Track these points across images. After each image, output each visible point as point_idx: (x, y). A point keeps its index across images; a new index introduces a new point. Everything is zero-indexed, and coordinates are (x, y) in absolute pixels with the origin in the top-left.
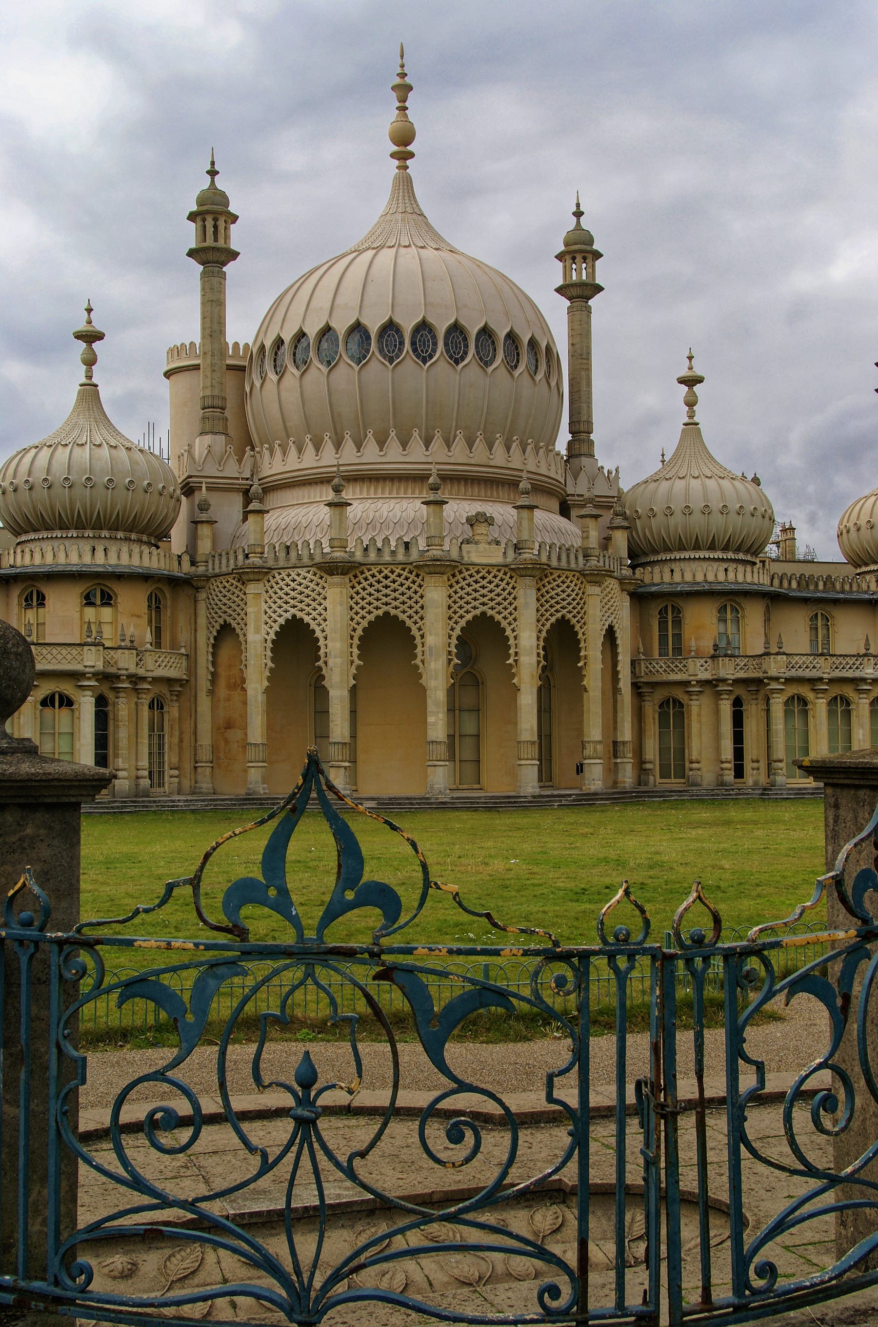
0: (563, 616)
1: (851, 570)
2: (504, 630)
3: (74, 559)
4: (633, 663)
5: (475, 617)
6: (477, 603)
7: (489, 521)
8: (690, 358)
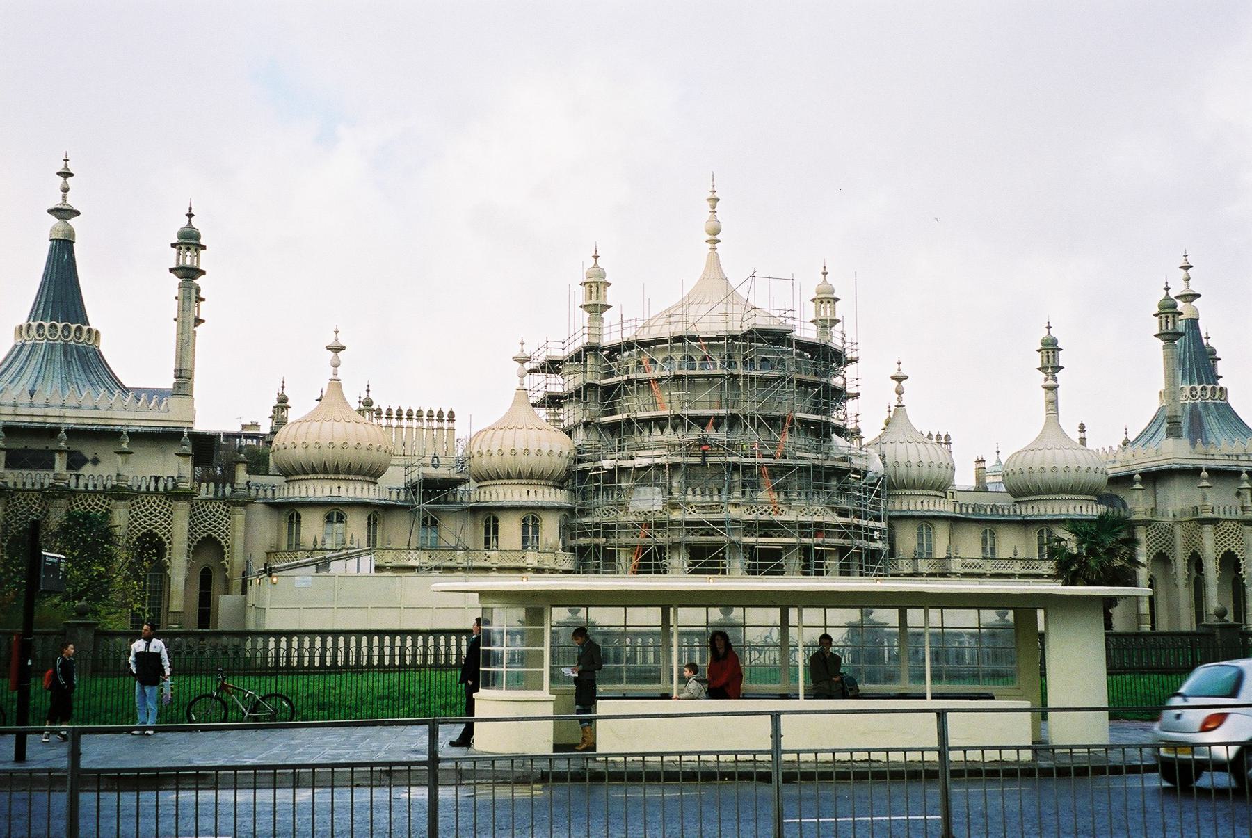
3: (517, 498)
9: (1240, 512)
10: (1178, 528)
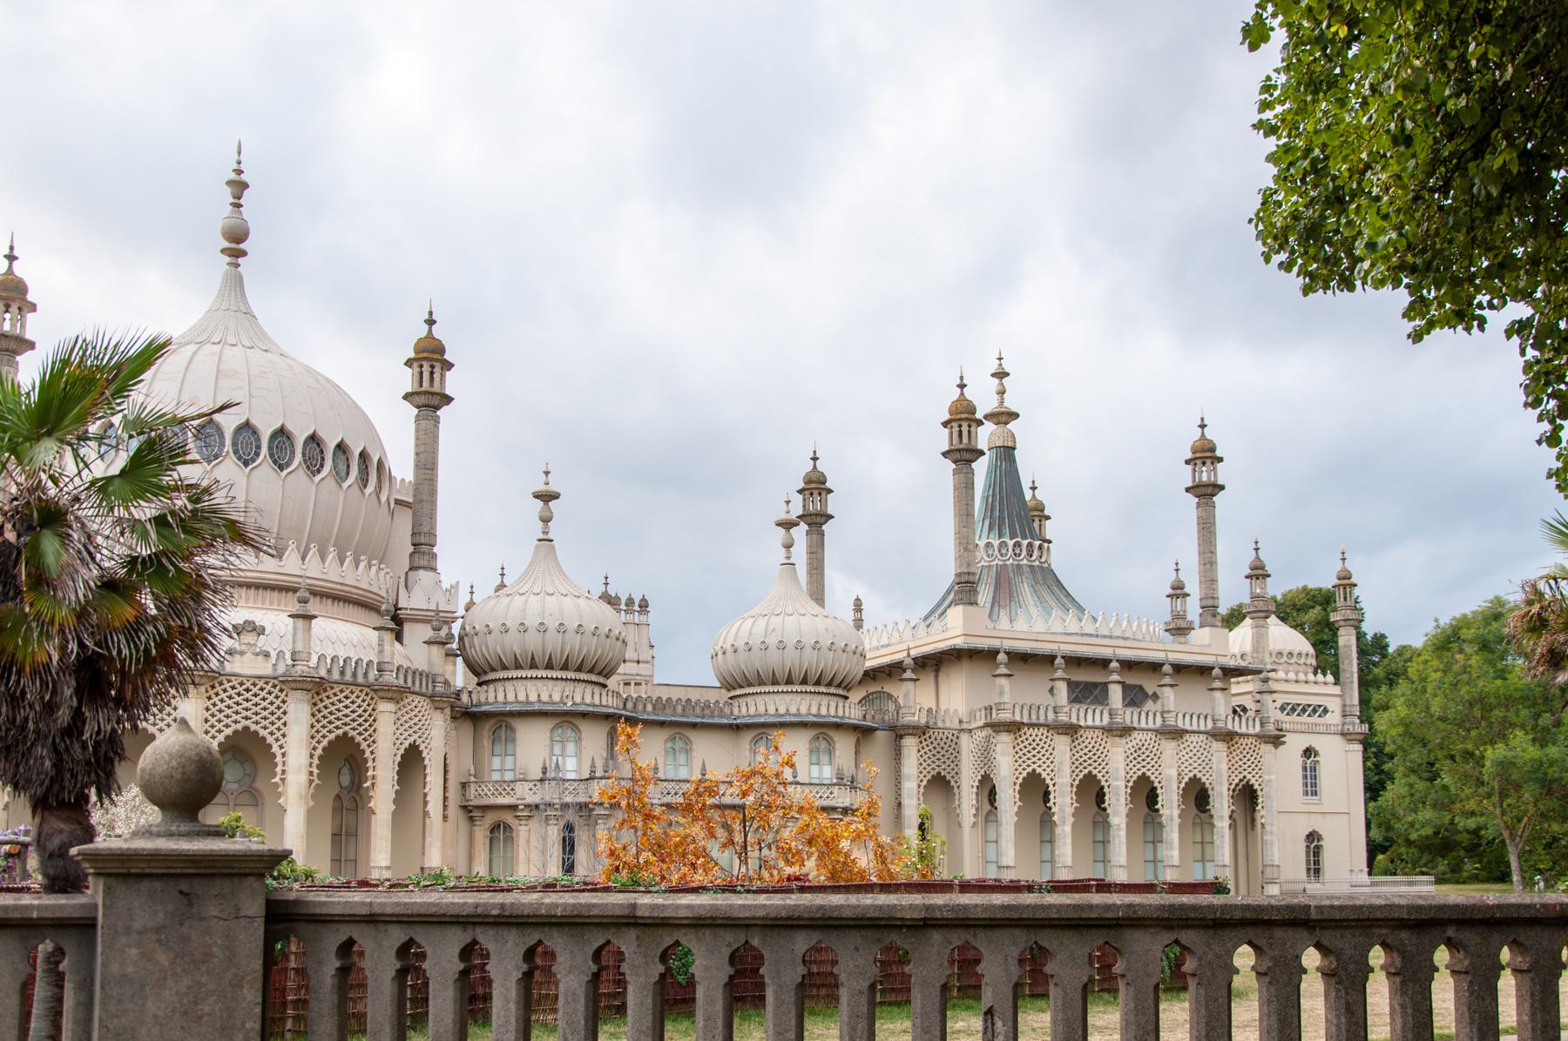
0: (345, 734)
1: (724, 695)
2: (270, 746)
4: (464, 785)
5: (236, 732)
6: (238, 717)
7: (259, 631)
8: (547, 473)
9: (1051, 716)
10: (964, 738)
